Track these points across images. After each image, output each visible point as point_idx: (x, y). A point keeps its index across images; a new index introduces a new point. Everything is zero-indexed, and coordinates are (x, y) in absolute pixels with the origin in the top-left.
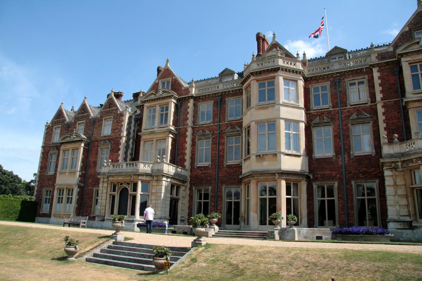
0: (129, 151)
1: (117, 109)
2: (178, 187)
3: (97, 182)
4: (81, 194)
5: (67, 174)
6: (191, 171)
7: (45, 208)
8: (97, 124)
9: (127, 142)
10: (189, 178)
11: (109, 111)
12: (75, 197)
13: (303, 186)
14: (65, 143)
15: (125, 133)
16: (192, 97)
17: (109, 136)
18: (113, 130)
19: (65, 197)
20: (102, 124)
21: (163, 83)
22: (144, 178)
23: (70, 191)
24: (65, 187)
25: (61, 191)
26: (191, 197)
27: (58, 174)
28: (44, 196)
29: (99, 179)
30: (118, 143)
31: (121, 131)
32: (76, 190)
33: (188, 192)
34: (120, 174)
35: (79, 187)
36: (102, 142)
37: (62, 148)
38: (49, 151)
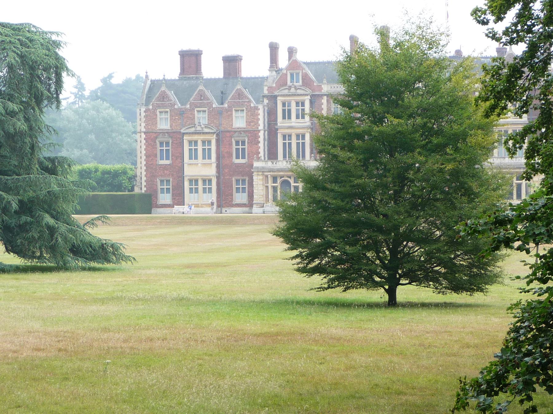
5: (199, 165)
7: (165, 198)
11: (239, 102)
14: (190, 133)
16: (325, 95)
17: (244, 128)
18: (248, 123)
19: (200, 186)
20: (232, 114)
21: (292, 75)
24: (199, 177)
25: (194, 181)
27: (186, 166)
28: (159, 187)
29: (253, 173)
31: (257, 124)
34: (279, 170)
36: (237, 134)
38: (156, 138)
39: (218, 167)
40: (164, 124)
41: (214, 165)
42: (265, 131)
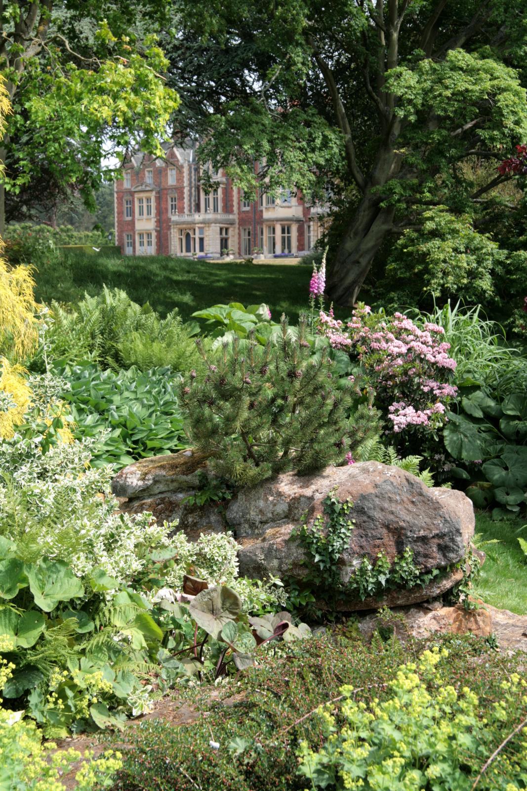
0: (193, 199)
1: (178, 161)
2: (227, 229)
3: (169, 228)
4: (159, 237)
6: (239, 214)
8: (163, 173)
9: (190, 191)
10: (237, 221)
12: (154, 240)
13: (294, 228)
15: (186, 183)
19: (145, 240)
22: (200, 225)
23: (149, 235)
26: (239, 234)
28: (126, 241)
30: (183, 193)
31: (183, 182)
32: (154, 234)
33: (237, 231)
34: (183, 223)
35: (156, 231)
37: (136, 196)
39: (159, 222)
40: (127, 185)
41: (154, 220)
42: (191, 188)
